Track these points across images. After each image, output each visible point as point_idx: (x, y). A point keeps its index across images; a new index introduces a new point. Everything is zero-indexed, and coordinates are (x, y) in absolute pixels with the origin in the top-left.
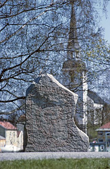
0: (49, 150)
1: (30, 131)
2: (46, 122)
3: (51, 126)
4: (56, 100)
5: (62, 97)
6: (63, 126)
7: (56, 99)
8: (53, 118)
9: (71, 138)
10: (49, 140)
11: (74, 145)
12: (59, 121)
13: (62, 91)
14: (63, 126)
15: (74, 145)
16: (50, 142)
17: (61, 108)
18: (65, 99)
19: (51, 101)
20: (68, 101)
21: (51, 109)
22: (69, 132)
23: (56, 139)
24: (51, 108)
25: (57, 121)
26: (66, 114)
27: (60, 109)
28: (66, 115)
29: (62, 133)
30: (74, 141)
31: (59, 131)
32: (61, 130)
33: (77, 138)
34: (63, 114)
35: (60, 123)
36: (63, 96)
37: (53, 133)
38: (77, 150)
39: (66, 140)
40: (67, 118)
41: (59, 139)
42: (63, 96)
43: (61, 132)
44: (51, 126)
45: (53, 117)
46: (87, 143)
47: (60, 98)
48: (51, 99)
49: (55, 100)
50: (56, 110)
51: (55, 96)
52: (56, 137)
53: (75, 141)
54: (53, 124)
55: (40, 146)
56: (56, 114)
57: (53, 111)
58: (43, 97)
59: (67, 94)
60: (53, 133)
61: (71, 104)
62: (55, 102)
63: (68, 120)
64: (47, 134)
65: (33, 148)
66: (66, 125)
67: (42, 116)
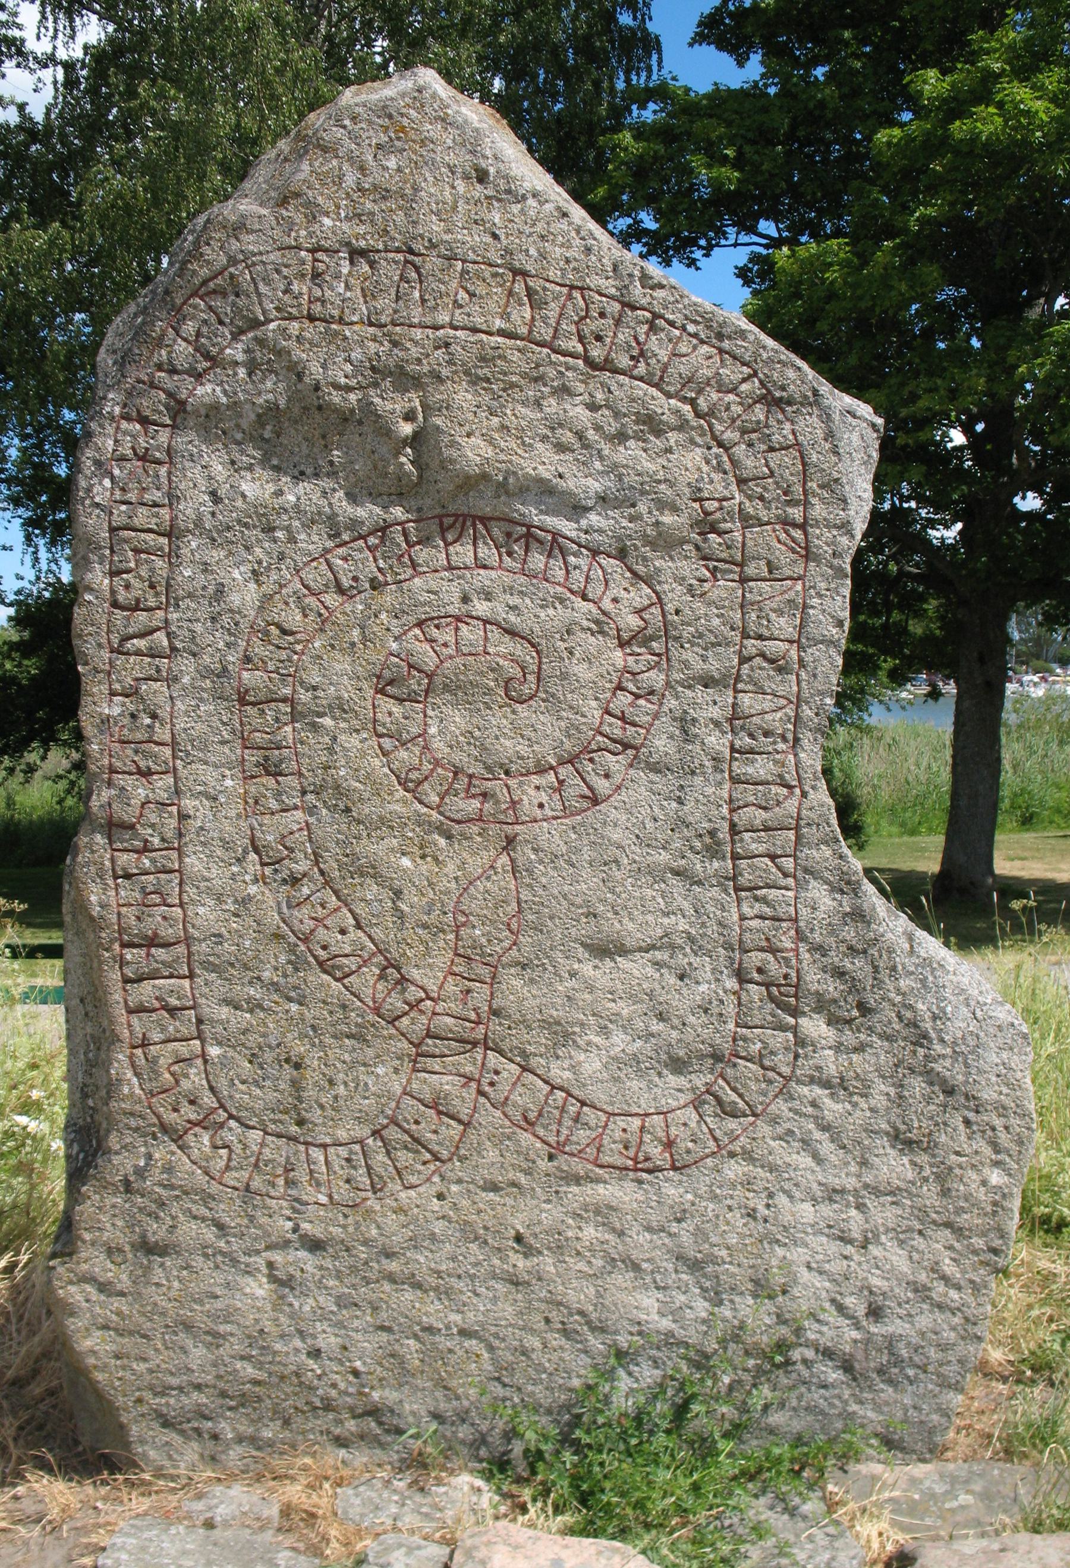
0: (438, 1227)
1: (152, 942)
2: (398, 804)
3: (476, 864)
4: (566, 463)
5: (653, 425)
6: (656, 873)
7: (561, 448)
8: (509, 746)
9: (780, 1039)
10: (448, 1083)
11: (826, 1148)
12: (602, 786)
13: (653, 328)
14: (656, 873)
15: (826, 1148)
16: (463, 1100)
17: (642, 595)
18: (697, 455)
19: (470, 483)
20: (741, 482)
21: (481, 608)
22: (756, 958)
23: (559, 1073)
24: (488, 597)
25: (575, 787)
26: (707, 682)
27: (625, 603)
28: (711, 707)
29: (637, 967)
30: (826, 1084)
31: (605, 950)
32: (631, 930)
33: (860, 1049)
34: (656, 679)
35: (617, 822)
36: (662, 405)
37: (513, 982)
38: (860, 1207)
39: (700, 1081)
40: (718, 742)
41: (592, 1064)
42: (662, 405)
43: (623, 951)
44: (476, 864)
45: (526, 733)
46: (1002, 1110)
47: (621, 437)
48: (474, 452)
49: (542, 463)
50: (556, 615)
51: (552, 406)
52: (562, 1035)
53: (838, 1086)
54: (511, 841)
55: (301, 1175)
56: (564, 676)
57: (512, 633)
58: (345, 418)
59: (732, 373)
60: (513, 982)
61: (787, 523)
62: (545, 491)
63: (738, 768)
64: (414, 993)
65: (207, 1198)
66: (713, 851)
67: (340, 708)
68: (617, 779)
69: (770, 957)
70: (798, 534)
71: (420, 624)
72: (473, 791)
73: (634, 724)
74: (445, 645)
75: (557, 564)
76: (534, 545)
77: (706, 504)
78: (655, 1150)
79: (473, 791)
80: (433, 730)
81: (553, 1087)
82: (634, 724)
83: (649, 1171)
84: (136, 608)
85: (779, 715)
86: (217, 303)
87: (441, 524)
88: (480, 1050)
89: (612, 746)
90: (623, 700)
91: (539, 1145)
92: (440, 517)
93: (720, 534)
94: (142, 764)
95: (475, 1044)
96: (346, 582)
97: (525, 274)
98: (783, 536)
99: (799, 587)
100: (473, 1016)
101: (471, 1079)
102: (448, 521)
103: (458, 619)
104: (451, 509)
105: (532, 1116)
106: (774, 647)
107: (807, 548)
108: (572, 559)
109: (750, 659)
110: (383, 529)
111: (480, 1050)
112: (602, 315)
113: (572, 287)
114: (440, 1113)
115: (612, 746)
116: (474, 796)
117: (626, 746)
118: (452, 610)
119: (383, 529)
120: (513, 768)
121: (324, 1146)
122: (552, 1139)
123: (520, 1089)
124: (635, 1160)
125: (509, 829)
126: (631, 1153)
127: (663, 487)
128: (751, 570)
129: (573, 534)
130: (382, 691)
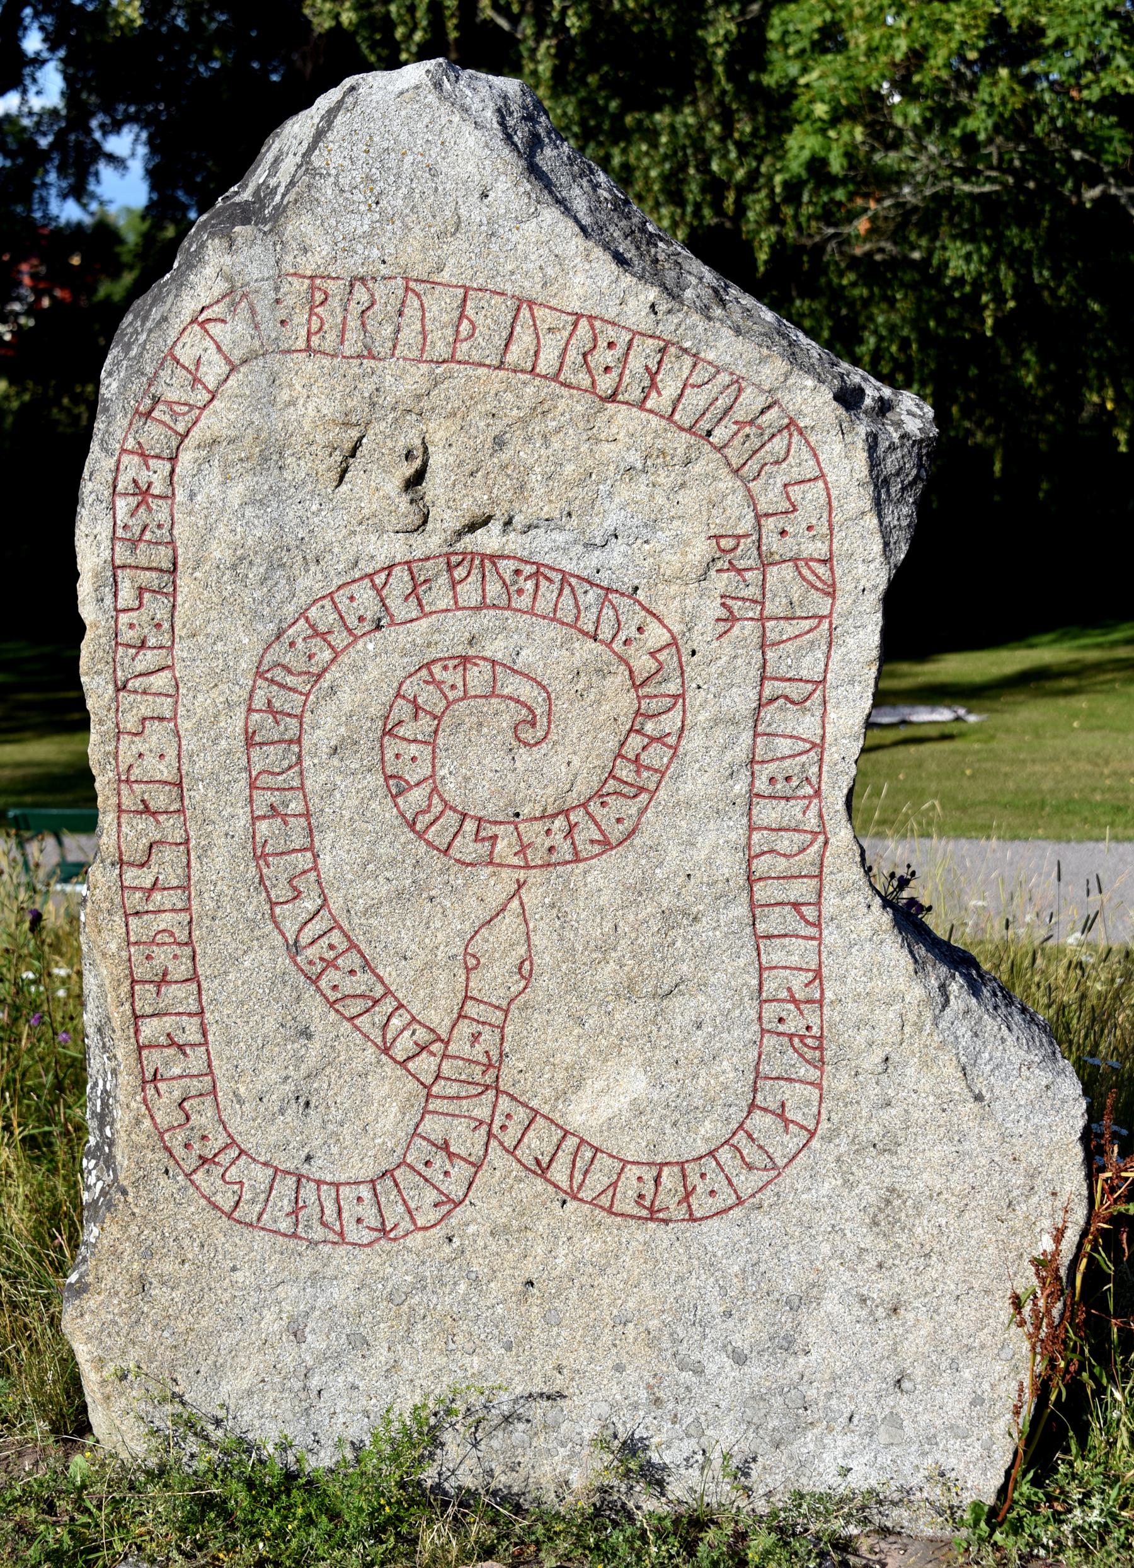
12: (616, 832)
64: (422, 1035)
68: (627, 825)
69: (791, 1006)
70: (821, 570)
71: (428, 665)
72: (483, 834)
73: (648, 768)
74: (453, 687)
75: (567, 600)
76: (543, 583)
77: (723, 542)
78: (668, 1200)
79: (483, 834)
80: (443, 772)
81: (566, 1132)
82: (648, 768)
83: (666, 1222)
84: (143, 645)
85: (804, 758)
86: (215, 329)
87: (448, 563)
88: (491, 1093)
89: (626, 790)
90: (636, 741)
91: (550, 1188)
92: (448, 555)
93: (739, 571)
94: (152, 806)
95: (487, 1087)
96: (352, 621)
97: (531, 303)
98: (805, 571)
99: (825, 625)
100: (485, 1061)
101: (481, 1123)
102: (454, 559)
103: (465, 660)
104: (459, 547)
105: (545, 1161)
106: (795, 691)
107: (834, 585)
108: (581, 598)
109: (771, 701)
110: (390, 568)
111: (491, 1093)
112: (611, 345)
113: (579, 316)
114: (451, 1155)
115: (626, 790)
116: (483, 839)
117: (642, 789)
118: (459, 650)
119: (390, 568)
120: (525, 811)
121: (337, 1185)
122: (565, 1185)
123: (531, 1134)
124: (651, 1209)
125: (522, 875)
126: (647, 1203)
127: (676, 523)
128: (770, 608)
129: (585, 574)
130: (389, 733)
